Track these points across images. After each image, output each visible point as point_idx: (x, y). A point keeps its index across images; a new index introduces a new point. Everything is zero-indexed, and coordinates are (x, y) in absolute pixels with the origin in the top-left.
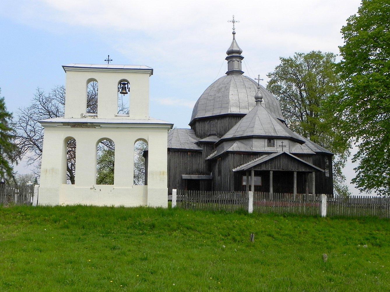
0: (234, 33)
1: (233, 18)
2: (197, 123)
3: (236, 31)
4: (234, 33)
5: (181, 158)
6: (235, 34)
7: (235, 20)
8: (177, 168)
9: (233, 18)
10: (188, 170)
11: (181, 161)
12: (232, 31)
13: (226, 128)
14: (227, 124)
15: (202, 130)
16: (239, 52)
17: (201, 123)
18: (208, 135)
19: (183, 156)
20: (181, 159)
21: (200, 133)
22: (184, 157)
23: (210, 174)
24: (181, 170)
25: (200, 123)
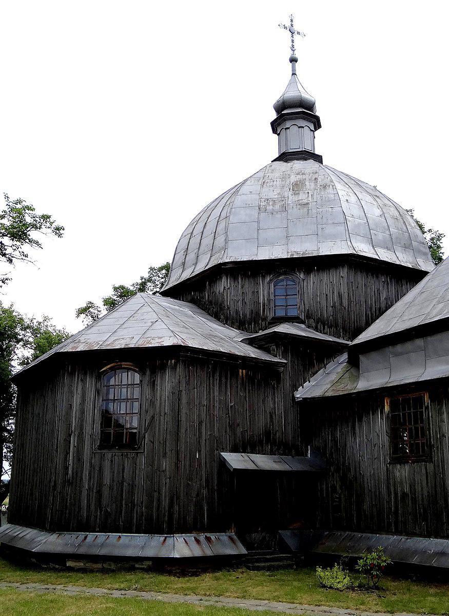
0: (293, 60)
1: (292, 21)
2: (224, 279)
3: (297, 55)
4: (293, 60)
5: (216, 388)
6: (296, 61)
7: (296, 28)
8: (204, 425)
9: (292, 21)
10: (239, 434)
11: (217, 398)
12: (289, 54)
13: (340, 296)
14: (344, 290)
15: (244, 303)
16: (310, 106)
17: (242, 279)
18: (271, 316)
19: (220, 380)
20: (216, 393)
21: (237, 312)
22: (226, 387)
23: (301, 453)
24: (216, 434)
25: (235, 278)
